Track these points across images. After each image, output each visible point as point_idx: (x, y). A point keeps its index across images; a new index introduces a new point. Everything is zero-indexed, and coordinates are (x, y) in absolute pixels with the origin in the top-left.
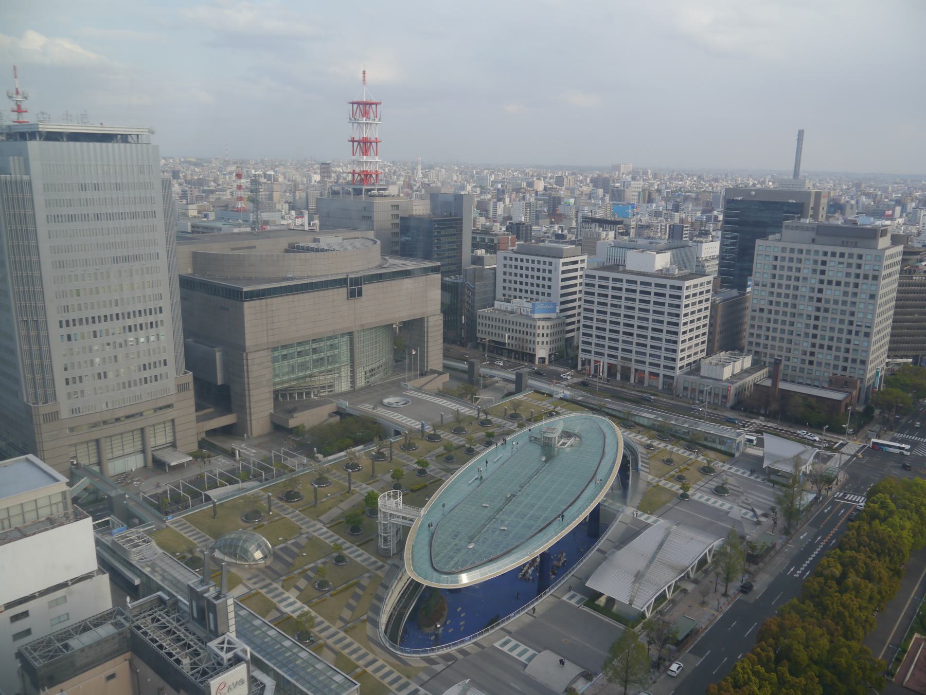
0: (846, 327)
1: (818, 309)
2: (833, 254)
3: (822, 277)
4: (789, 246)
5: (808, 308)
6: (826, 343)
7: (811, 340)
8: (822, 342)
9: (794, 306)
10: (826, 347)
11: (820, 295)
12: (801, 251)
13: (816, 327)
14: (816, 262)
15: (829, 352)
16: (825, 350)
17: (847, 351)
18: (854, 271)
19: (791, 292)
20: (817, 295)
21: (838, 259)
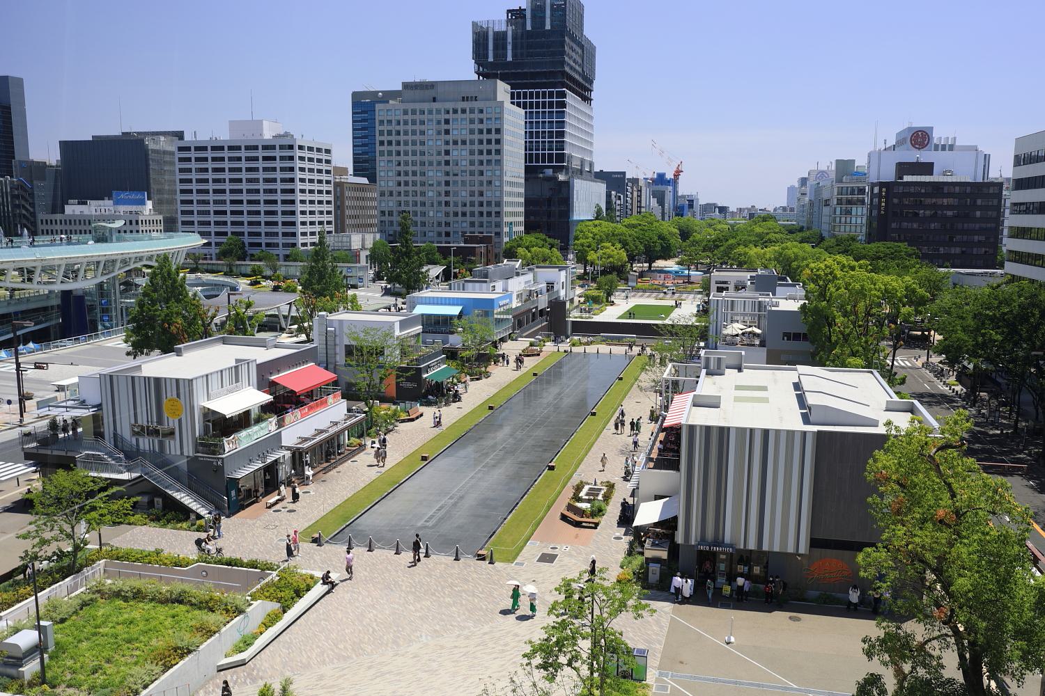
0: (477, 199)
1: (447, 174)
2: (455, 111)
3: (447, 137)
4: (410, 106)
5: (436, 175)
6: (460, 209)
7: (443, 208)
8: (455, 209)
9: (423, 174)
10: (460, 214)
11: (447, 158)
12: (423, 112)
13: (447, 194)
14: (439, 122)
15: (464, 218)
16: (460, 218)
17: (481, 204)
18: (477, 126)
19: (418, 158)
20: (444, 158)
21: (459, 115)
